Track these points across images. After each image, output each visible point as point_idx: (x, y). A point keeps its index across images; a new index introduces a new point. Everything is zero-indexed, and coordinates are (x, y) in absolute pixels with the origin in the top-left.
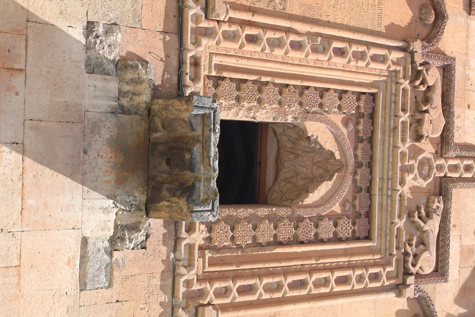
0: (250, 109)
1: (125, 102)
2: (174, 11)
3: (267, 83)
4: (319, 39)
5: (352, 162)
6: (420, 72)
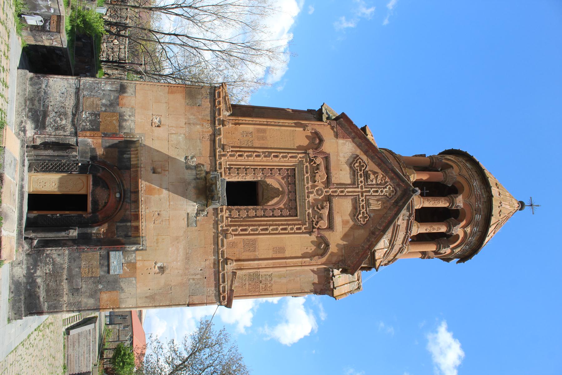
1: (198, 176)
5: (287, 191)
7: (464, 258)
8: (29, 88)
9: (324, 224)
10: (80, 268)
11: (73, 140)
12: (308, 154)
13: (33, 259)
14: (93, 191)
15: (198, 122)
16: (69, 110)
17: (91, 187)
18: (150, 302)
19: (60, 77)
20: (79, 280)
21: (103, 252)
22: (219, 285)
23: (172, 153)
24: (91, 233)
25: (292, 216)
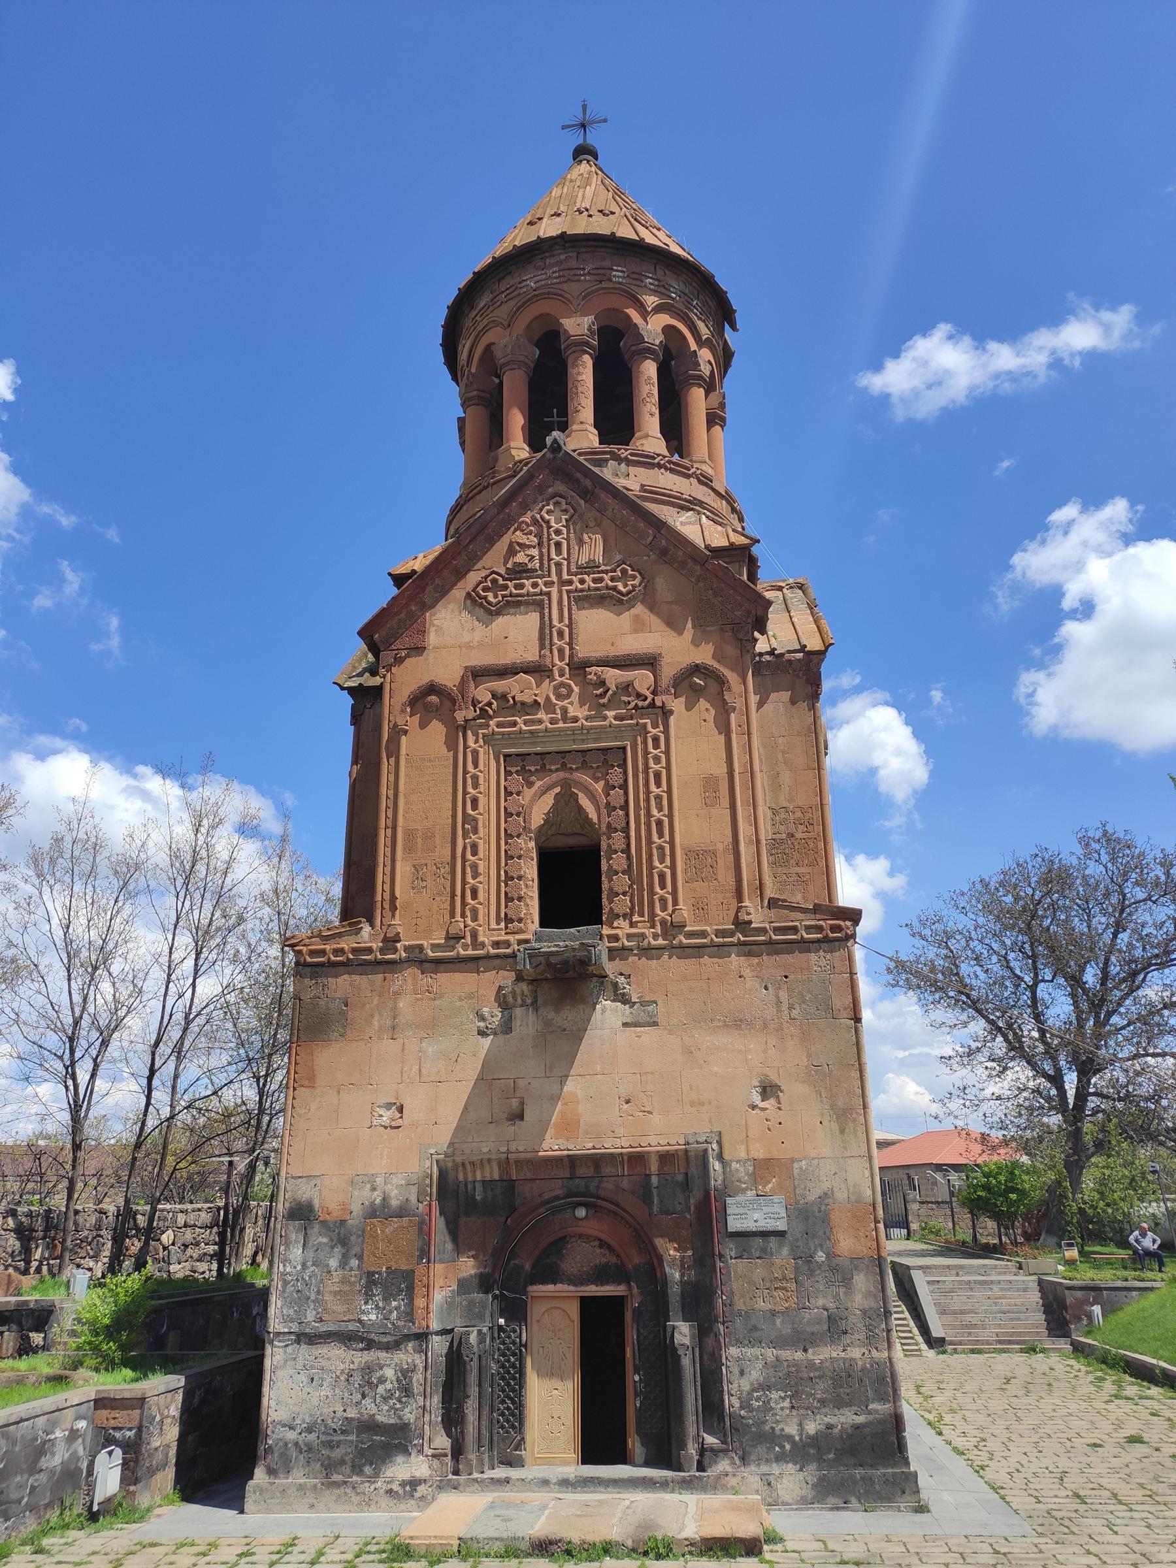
0: (527, 886)
1: (529, 1001)
2: (463, 964)
3: (506, 872)
4: (467, 826)
5: (562, 774)
6: (481, 709)
7: (722, 312)
8: (298, 1477)
9: (642, 679)
10: (774, 1313)
11: (439, 1345)
12: (466, 721)
13: (755, 1446)
14: (571, 1282)
15: (390, 1004)
16: (357, 1361)
17: (559, 1287)
18: (854, 1120)
19: (266, 1390)
20: (806, 1315)
21: (730, 1249)
22: (803, 941)
23: (471, 1070)
24: (682, 1283)
25: (625, 760)
